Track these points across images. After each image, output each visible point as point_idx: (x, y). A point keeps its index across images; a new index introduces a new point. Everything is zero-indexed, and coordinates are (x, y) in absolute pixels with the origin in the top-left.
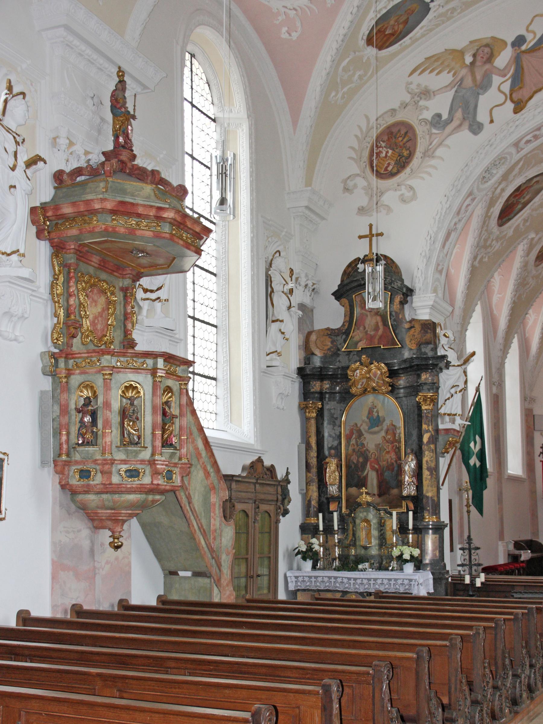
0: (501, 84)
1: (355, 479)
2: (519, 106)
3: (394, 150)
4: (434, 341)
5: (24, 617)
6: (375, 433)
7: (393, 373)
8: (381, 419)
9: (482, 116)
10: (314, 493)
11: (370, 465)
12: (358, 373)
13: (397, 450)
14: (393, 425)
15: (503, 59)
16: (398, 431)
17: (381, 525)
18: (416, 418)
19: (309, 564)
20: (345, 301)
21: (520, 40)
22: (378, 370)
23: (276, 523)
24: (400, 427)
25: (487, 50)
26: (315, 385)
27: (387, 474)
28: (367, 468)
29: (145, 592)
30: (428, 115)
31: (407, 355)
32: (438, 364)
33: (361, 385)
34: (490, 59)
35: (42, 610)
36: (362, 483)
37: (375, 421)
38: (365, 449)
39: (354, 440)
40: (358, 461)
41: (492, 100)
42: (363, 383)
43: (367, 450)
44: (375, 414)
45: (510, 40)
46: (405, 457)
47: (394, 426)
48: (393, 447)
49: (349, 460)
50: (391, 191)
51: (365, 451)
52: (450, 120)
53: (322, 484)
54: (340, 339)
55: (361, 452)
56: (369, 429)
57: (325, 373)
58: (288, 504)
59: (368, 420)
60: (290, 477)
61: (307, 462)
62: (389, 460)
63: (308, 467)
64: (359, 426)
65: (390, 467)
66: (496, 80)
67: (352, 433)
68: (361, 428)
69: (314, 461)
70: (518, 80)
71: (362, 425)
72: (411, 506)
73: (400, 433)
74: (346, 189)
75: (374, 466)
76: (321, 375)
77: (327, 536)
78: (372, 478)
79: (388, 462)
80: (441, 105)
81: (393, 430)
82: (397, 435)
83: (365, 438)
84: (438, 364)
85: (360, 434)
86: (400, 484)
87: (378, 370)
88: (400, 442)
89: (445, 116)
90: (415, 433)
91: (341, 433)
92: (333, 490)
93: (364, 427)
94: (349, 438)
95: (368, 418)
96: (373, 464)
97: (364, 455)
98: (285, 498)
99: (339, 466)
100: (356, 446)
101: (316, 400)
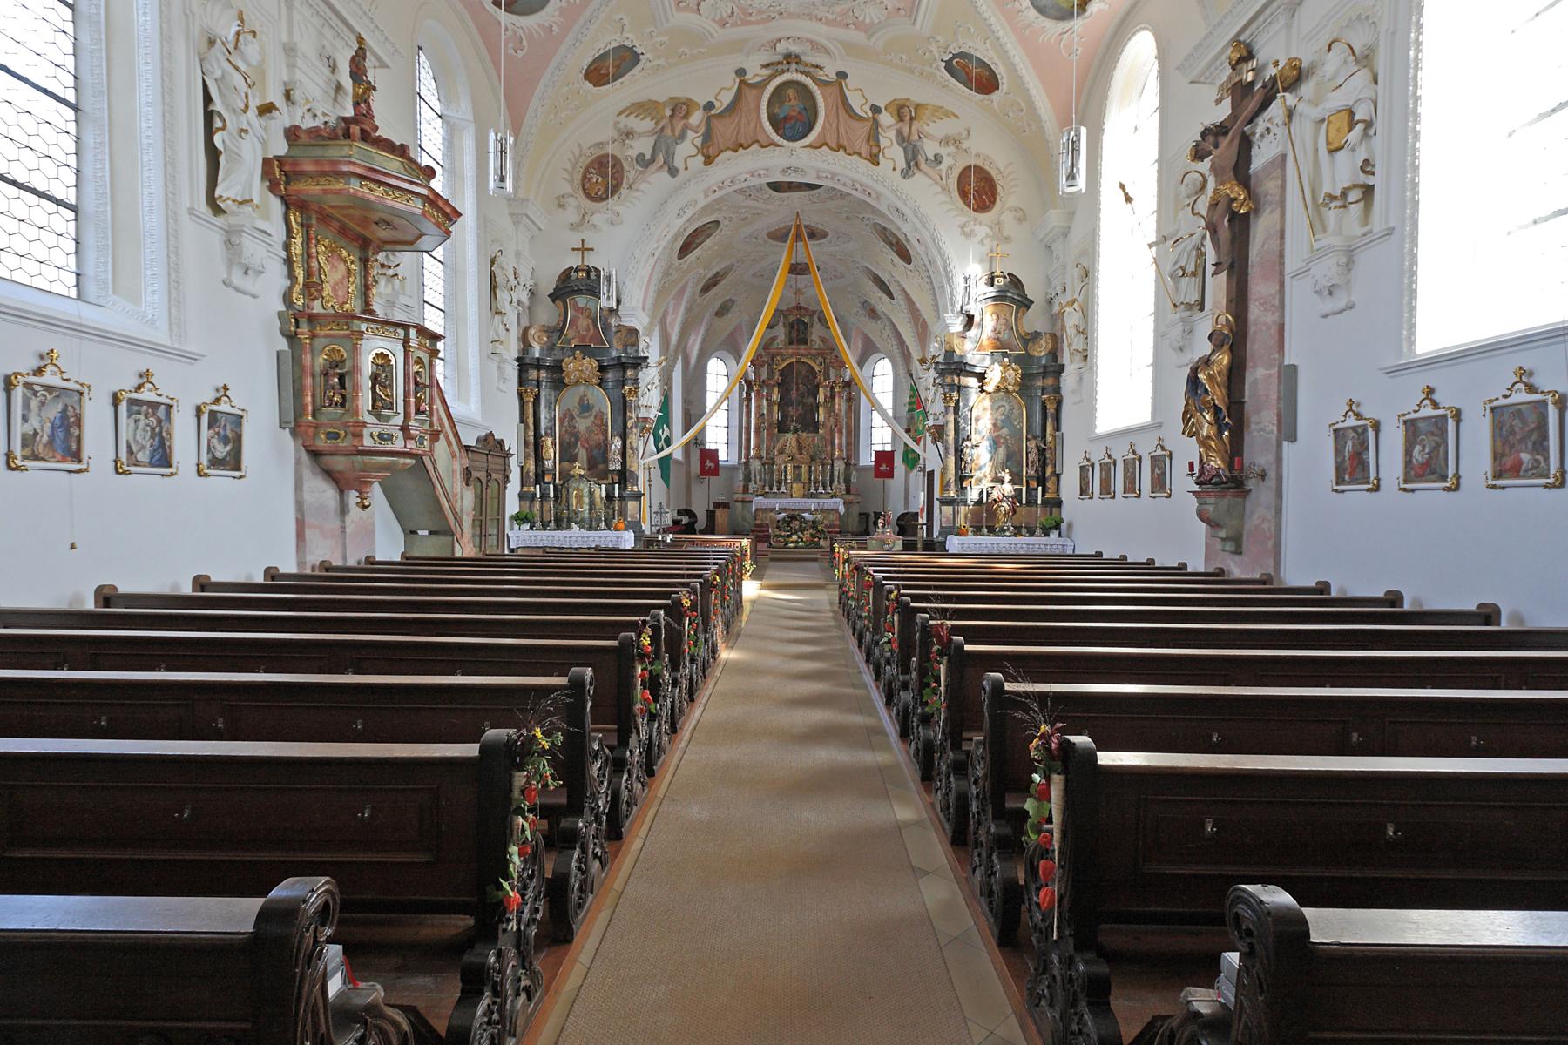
0: (694, 138)
1: (568, 455)
2: (709, 160)
3: (602, 178)
4: (636, 344)
5: (271, 573)
7: (602, 369)
9: (678, 163)
12: (570, 366)
15: (697, 118)
17: (591, 493)
18: (623, 406)
19: (527, 526)
20: (559, 303)
21: (709, 106)
22: (589, 365)
25: (681, 108)
27: (595, 452)
29: (389, 547)
30: (633, 153)
31: (614, 354)
32: (639, 362)
34: (687, 116)
35: (288, 566)
36: (573, 459)
37: (585, 408)
41: (686, 150)
45: (703, 103)
50: (601, 214)
52: (653, 160)
53: (539, 458)
54: (555, 336)
63: (526, 443)
65: (598, 446)
66: (690, 134)
70: (707, 137)
72: (616, 479)
74: (561, 206)
76: (538, 365)
78: (583, 454)
80: (643, 146)
84: (639, 362)
85: (572, 418)
86: (606, 461)
87: (589, 365)
89: (648, 157)
90: (620, 419)
92: (548, 464)
93: (576, 413)
94: (562, 421)
97: (576, 436)
99: (554, 443)
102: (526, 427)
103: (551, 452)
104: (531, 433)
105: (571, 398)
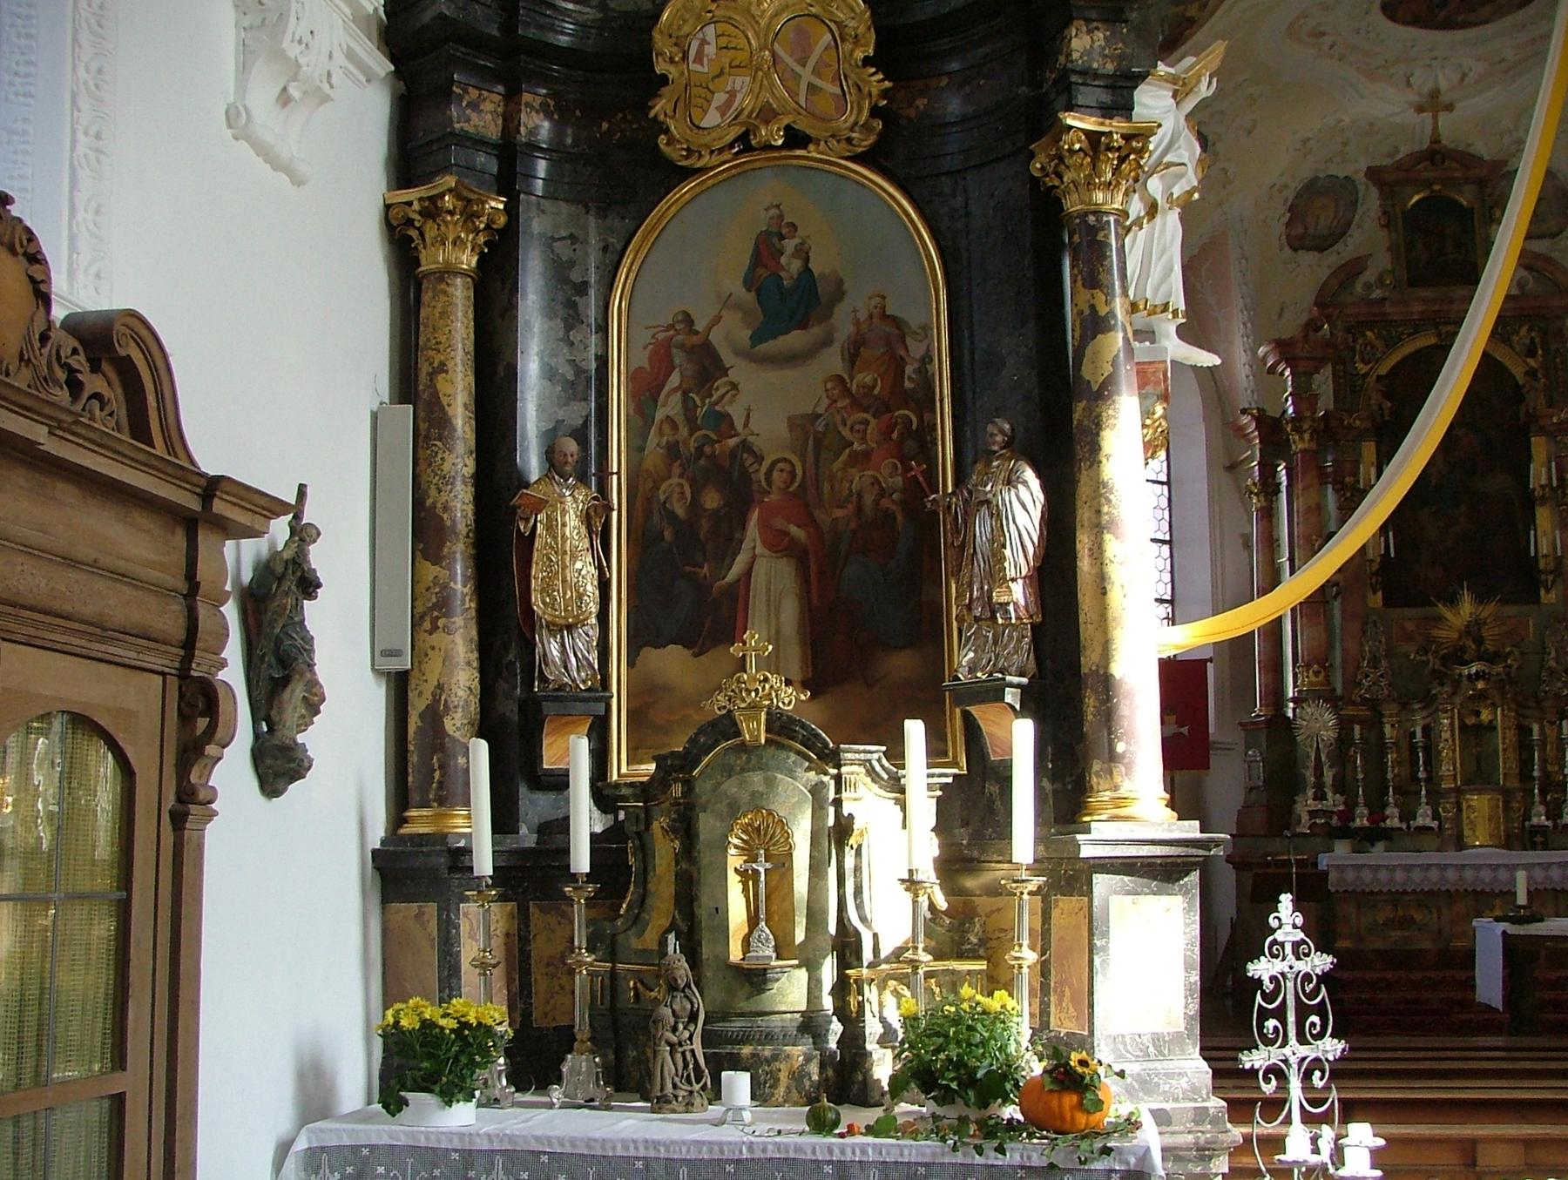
1: (678, 597)
6: (791, 359)
8: (823, 290)
10: (458, 673)
11: (764, 524)
13: (910, 444)
14: (884, 317)
16: (916, 349)
23: (179, 820)
24: (926, 328)
26: (474, 106)
28: (747, 545)
33: (723, 110)
37: (787, 300)
38: (732, 442)
39: (676, 399)
40: (695, 506)
42: (732, 94)
43: (745, 446)
44: (791, 266)
46: (959, 480)
47: (895, 321)
48: (891, 428)
49: (649, 500)
51: (733, 453)
55: (712, 457)
56: (757, 338)
57: (532, 33)
58: (305, 724)
59: (751, 297)
60: (318, 558)
61: (418, 503)
62: (869, 499)
63: (427, 531)
64: (700, 326)
67: (662, 360)
68: (716, 337)
69: (460, 503)
71: (717, 320)
73: (927, 359)
75: (787, 533)
77: (523, 916)
79: (859, 509)
81: (888, 343)
82: (909, 370)
83: (734, 386)
85: (708, 367)
88: (926, 401)
90: (1014, 350)
91: (603, 361)
92: (564, 656)
93: (729, 334)
94: (645, 393)
95: (749, 283)
96: (779, 523)
97: (728, 475)
98: (285, 682)
99: (596, 524)
100: (684, 431)
101: (481, 184)
102: (430, 427)
103: (576, 567)
104: (460, 461)
105: (689, 262)
